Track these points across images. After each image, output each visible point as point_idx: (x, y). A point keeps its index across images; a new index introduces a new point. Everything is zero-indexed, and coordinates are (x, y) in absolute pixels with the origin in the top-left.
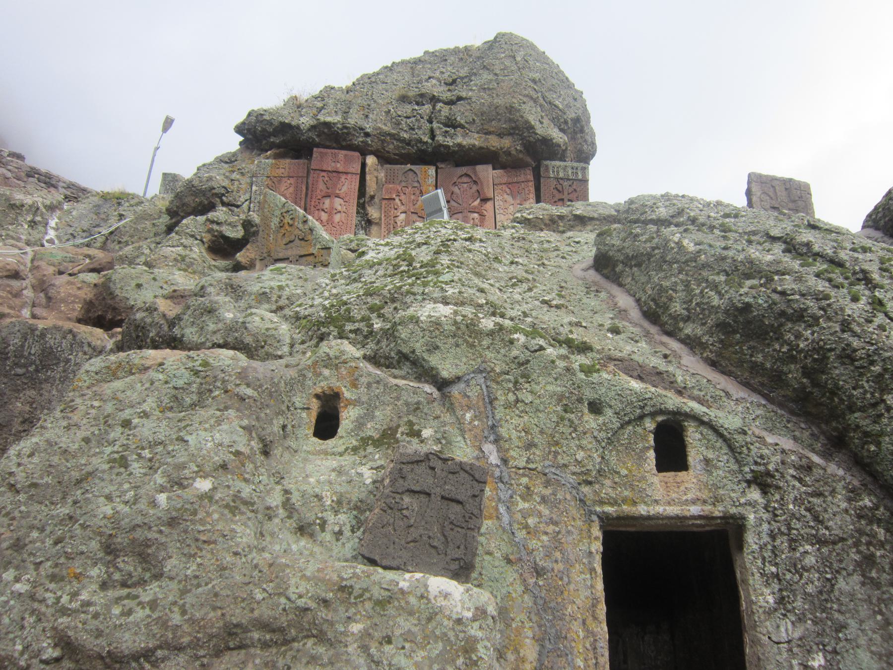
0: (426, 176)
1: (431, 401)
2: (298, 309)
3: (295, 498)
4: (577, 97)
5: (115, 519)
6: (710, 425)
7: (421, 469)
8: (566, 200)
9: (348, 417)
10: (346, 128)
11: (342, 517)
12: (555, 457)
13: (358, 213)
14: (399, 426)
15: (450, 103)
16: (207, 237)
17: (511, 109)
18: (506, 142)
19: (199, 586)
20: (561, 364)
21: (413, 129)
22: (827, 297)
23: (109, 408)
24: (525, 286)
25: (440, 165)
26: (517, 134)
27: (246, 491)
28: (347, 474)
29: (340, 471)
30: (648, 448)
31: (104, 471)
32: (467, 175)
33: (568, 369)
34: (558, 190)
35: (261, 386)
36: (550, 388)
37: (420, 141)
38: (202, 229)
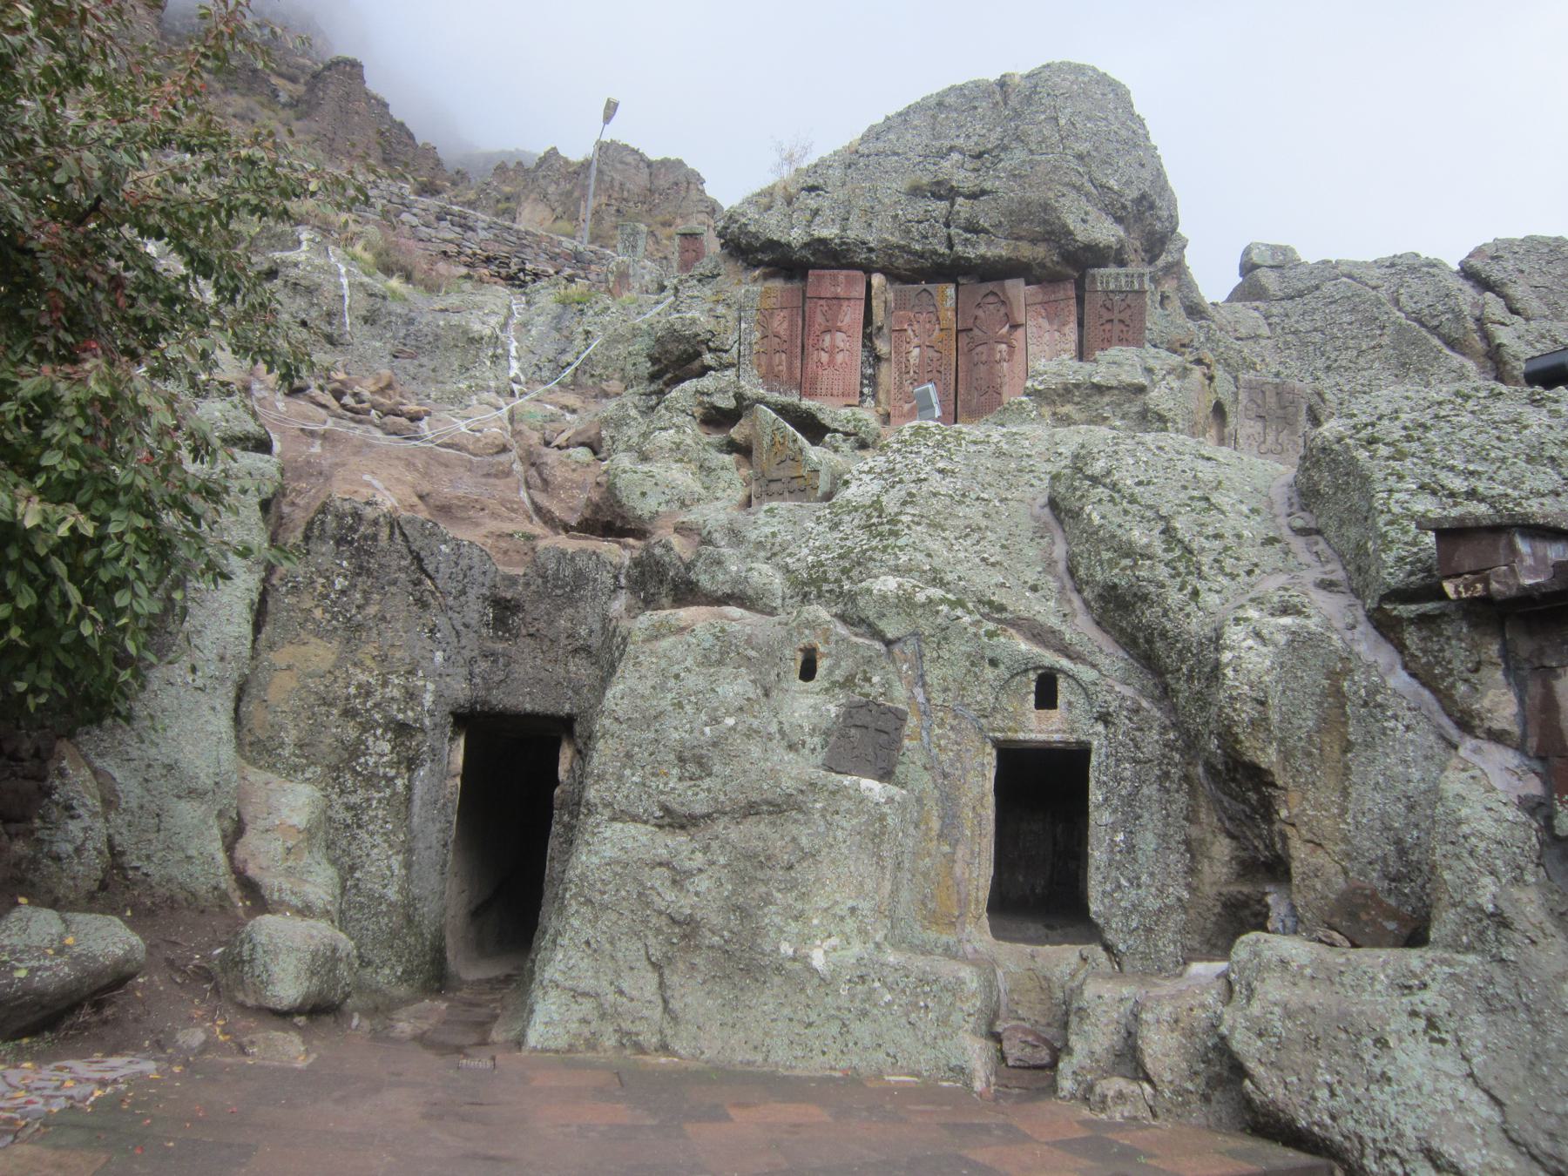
0: (944, 297)
1: (879, 656)
2: (788, 560)
3: (786, 727)
5: (682, 741)
6: (1072, 677)
7: (864, 711)
9: (823, 665)
11: (816, 739)
13: (864, 346)
15: (973, 196)
16: (698, 411)
17: (1046, 207)
20: (972, 630)
22: (1163, 586)
23: (663, 664)
24: (976, 536)
25: (961, 281)
27: (756, 723)
29: (815, 708)
32: (993, 293)
33: (975, 635)
37: (935, 252)
38: (691, 401)
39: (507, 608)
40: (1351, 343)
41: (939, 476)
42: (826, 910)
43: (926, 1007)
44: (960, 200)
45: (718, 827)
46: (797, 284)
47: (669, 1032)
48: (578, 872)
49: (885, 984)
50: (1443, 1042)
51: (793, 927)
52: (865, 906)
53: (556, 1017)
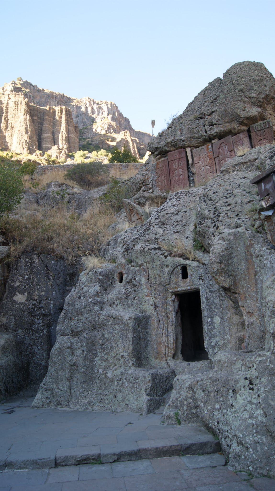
3: (109, 299)
9: (125, 276)
15: (210, 115)
25: (213, 142)
27: (99, 299)
37: (202, 136)
42: (114, 357)
50: (252, 389)
51: (104, 364)
52: (125, 354)
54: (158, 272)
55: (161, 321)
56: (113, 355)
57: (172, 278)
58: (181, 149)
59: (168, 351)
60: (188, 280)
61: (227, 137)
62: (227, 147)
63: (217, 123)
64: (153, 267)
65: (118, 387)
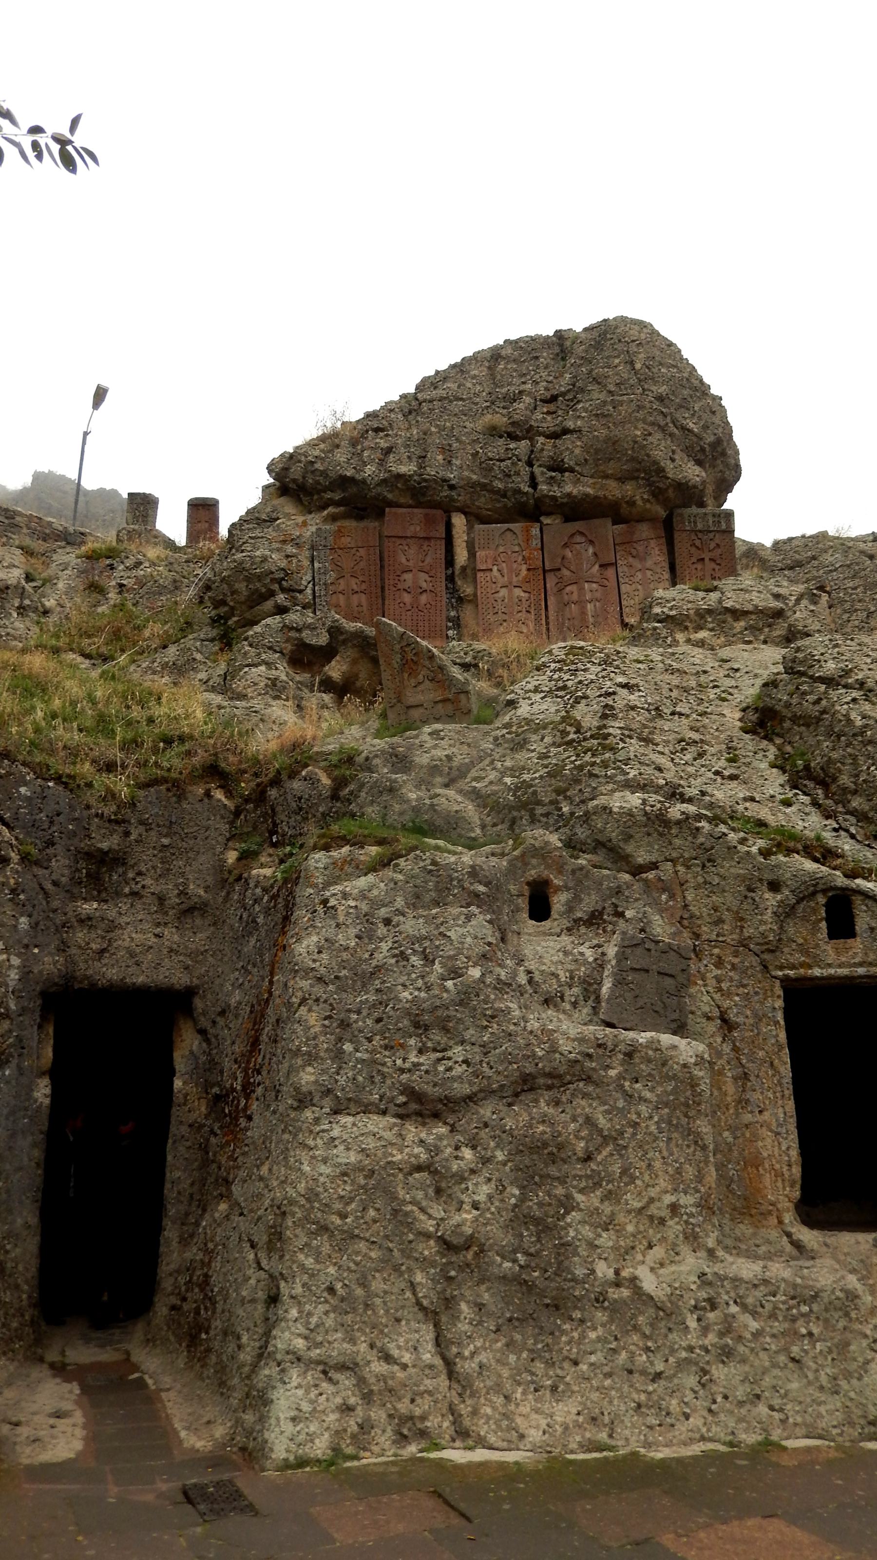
2: (474, 784)
3: (537, 977)
4: (715, 408)
7: (639, 951)
8: (707, 560)
9: (559, 901)
10: (426, 480)
11: (576, 990)
12: (742, 931)
13: (447, 588)
14: (604, 908)
15: (555, 436)
18: (629, 488)
19: (495, 1048)
21: (509, 476)
23: (364, 907)
24: (692, 751)
25: (546, 520)
26: (643, 478)
28: (571, 953)
30: (821, 920)
31: (391, 965)
34: (697, 547)
35: (490, 883)
36: (732, 870)
37: (518, 491)
39: (102, 862)
40: (858, 606)
41: (625, 692)
42: (640, 1211)
43: (810, 1334)
44: (541, 439)
45: (486, 1111)
46: (372, 524)
47: (464, 1409)
48: (302, 1187)
49: (744, 1307)
51: (606, 1240)
53: (306, 1407)
54: (731, 900)
55: (752, 1078)
56: (637, 1205)
57: (791, 930)
58: (434, 511)
59: (784, 1188)
60: (857, 945)
61: (597, 522)
62: (591, 550)
63: (577, 468)
64: (705, 883)
65: (711, 1338)
